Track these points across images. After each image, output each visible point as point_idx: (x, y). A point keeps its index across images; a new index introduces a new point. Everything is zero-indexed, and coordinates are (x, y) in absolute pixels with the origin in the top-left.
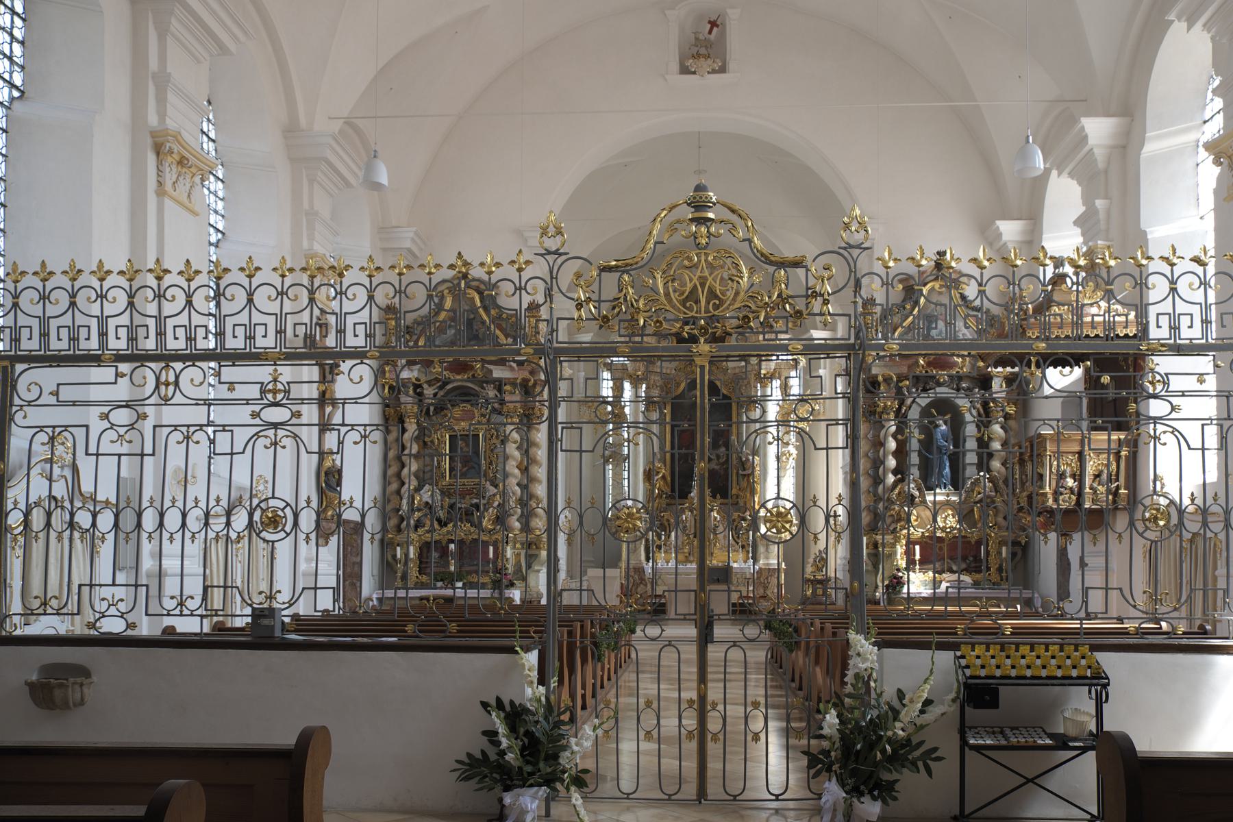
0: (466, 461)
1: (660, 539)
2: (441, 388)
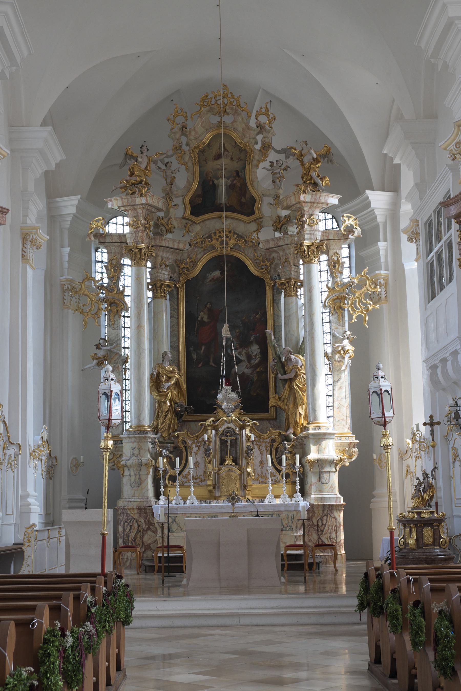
1: (173, 466)
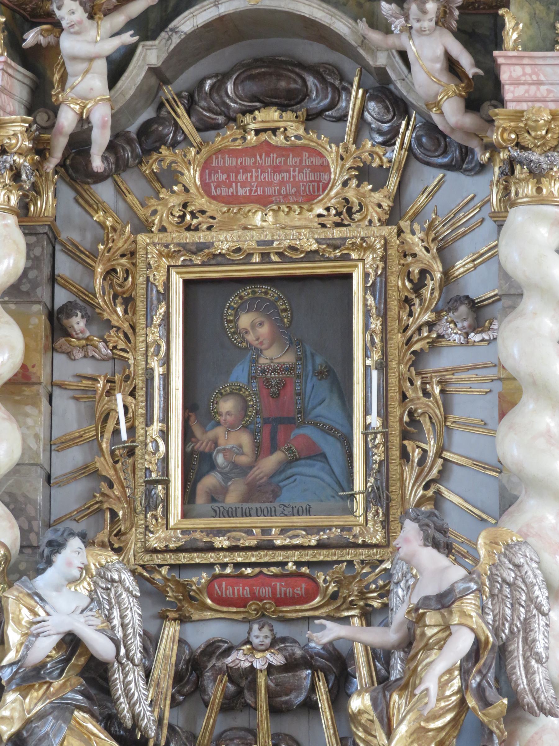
0: (274, 426)
2: (148, 26)
